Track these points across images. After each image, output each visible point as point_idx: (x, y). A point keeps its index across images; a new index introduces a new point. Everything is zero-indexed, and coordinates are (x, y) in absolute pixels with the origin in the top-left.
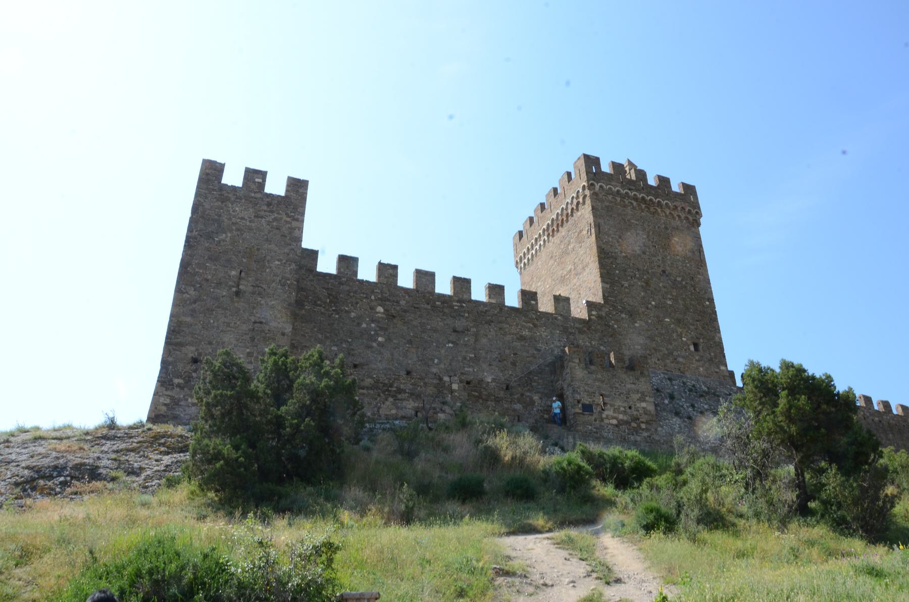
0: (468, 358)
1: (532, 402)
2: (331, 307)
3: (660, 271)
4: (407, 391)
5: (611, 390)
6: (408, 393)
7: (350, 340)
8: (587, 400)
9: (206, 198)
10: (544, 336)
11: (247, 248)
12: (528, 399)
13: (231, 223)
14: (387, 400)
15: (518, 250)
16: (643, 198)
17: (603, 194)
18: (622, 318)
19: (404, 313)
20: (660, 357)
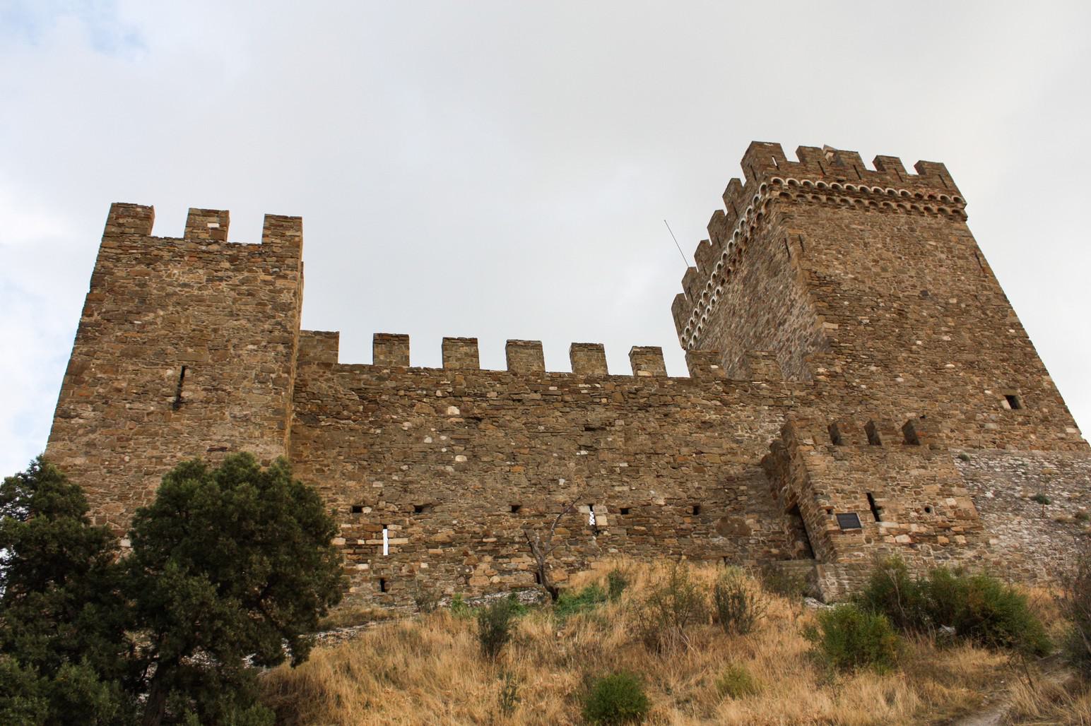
0: (618, 470)
1: (745, 531)
2: (367, 417)
3: (917, 292)
4: (517, 539)
5: (884, 483)
6: (518, 543)
7: (405, 467)
8: (843, 507)
9: (118, 260)
10: (742, 417)
11: (194, 330)
12: (736, 526)
13: (164, 294)
14: (480, 560)
17: (797, 193)
18: (872, 373)
19: (495, 412)
20: (953, 427)
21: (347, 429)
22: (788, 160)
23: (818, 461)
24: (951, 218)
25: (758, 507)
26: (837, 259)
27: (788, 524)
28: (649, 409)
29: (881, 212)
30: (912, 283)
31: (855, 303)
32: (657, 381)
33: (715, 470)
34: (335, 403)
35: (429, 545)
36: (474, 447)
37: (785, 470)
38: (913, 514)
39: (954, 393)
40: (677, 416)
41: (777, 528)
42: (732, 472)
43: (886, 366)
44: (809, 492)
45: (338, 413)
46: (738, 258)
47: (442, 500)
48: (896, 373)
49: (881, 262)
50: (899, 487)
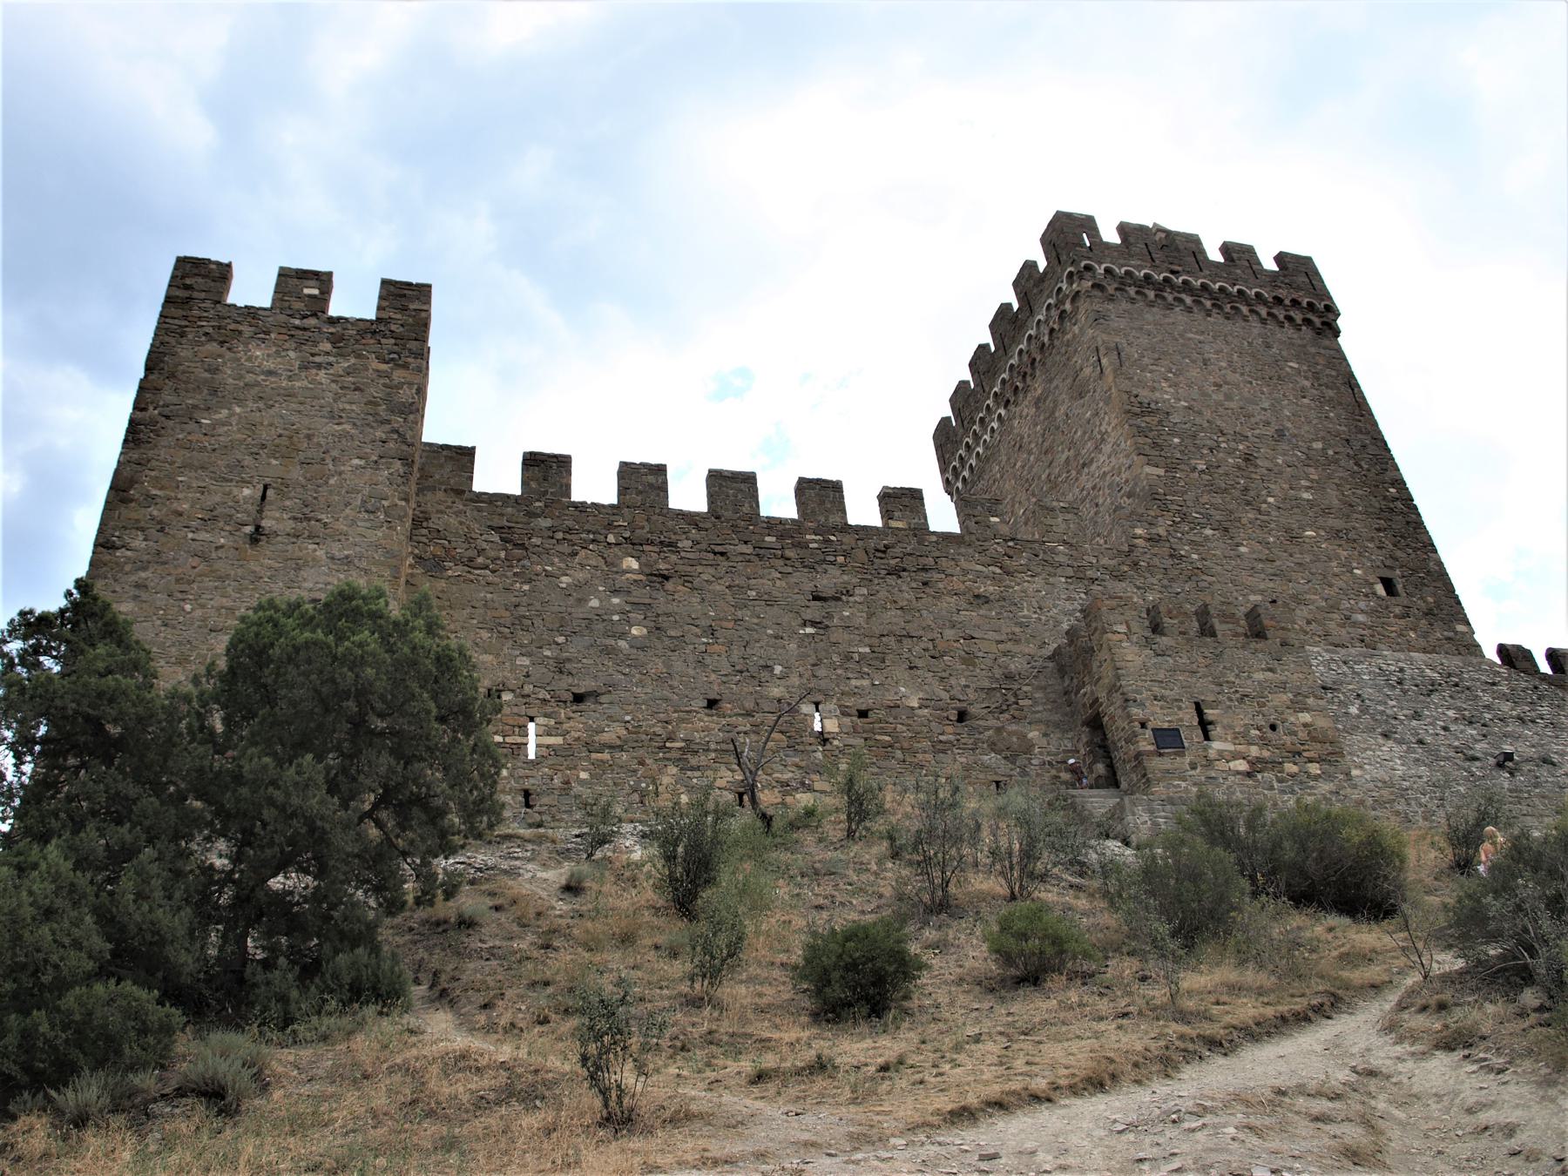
0: (856, 657)
1: (1028, 748)
3: (1270, 431)
4: (713, 746)
5: (1218, 689)
6: (716, 750)
7: (561, 639)
8: (1161, 718)
12: (1015, 739)
16: (1204, 287)
18: (1207, 538)
19: (689, 569)
20: (1310, 617)
21: (483, 582)
22: (1105, 239)
23: (1132, 655)
24: (1319, 332)
25: (1045, 715)
26: (1166, 380)
27: (1085, 740)
28: (902, 574)
29: (1228, 318)
34: (466, 546)
35: (589, 747)
36: (658, 615)
37: (1085, 666)
38: (1254, 732)
39: (1314, 570)
40: (941, 585)
41: (1069, 745)
42: (1012, 666)
44: (1117, 697)
45: (471, 560)
46: (1029, 371)
47: (611, 687)
49: (1225, 388)
50: (1238, 695)
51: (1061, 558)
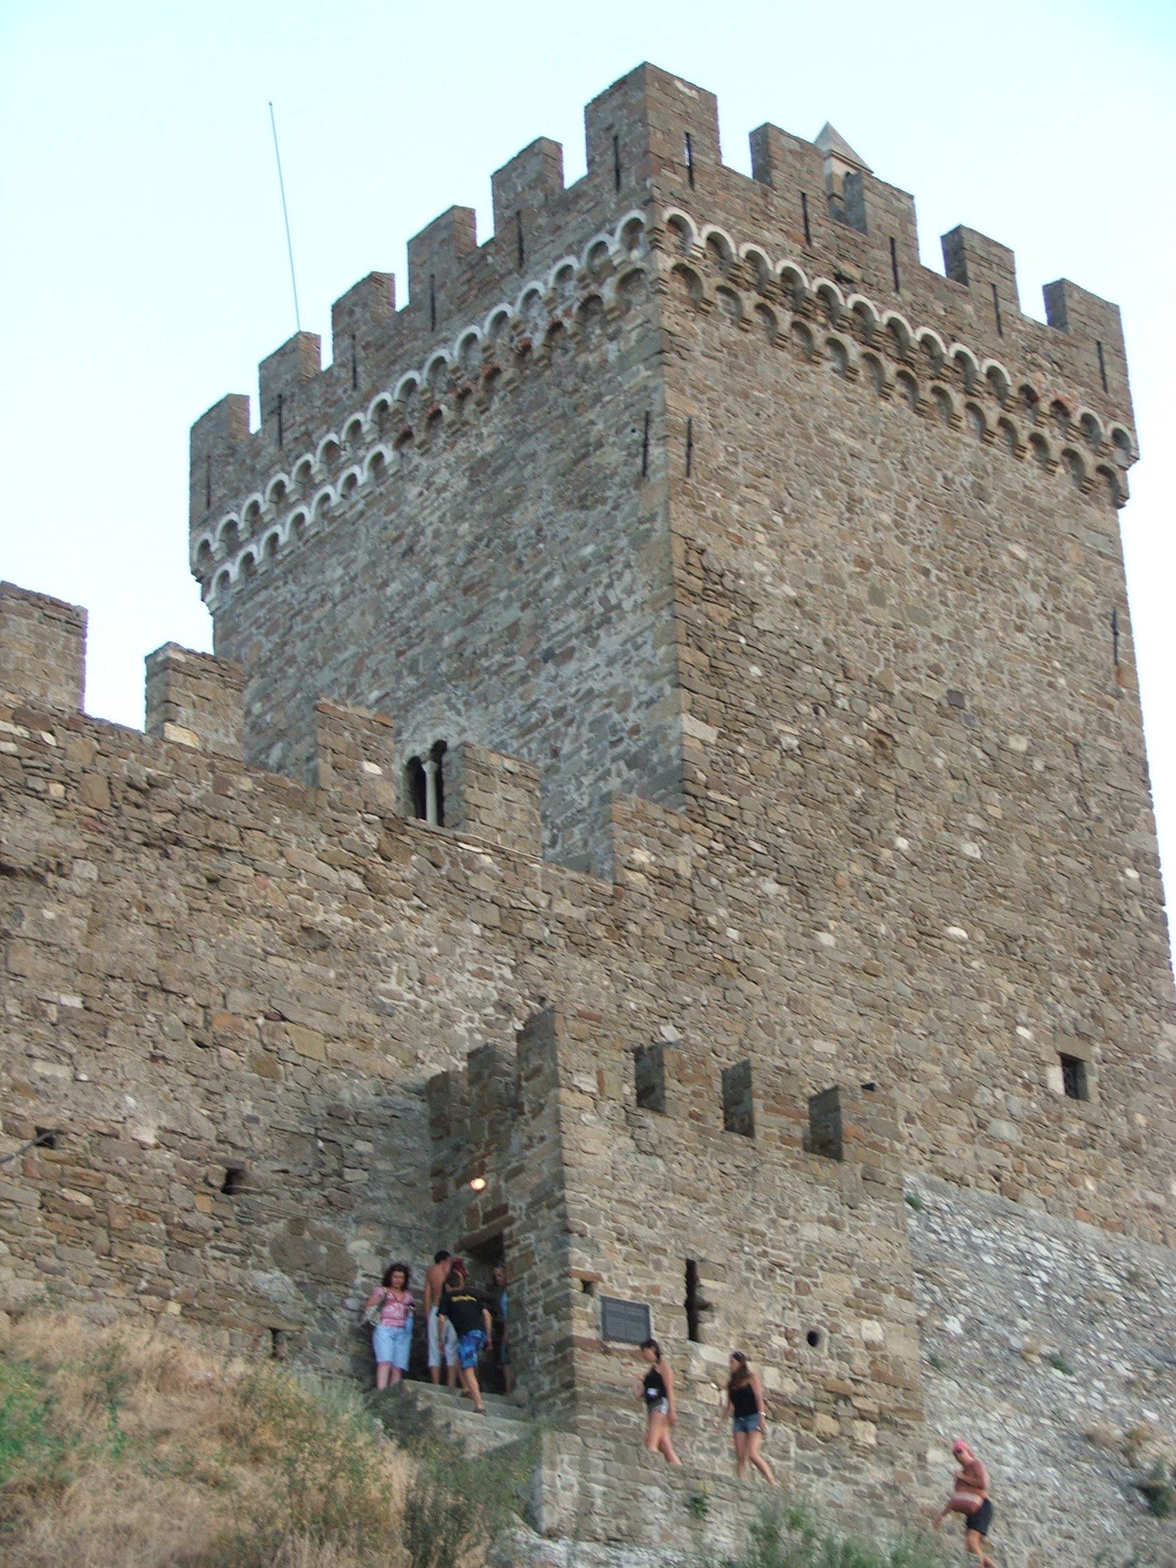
3: (937, 692)
5: (733, 1243)
12: (323, 1250)
15: (219, 492)
18: (764, 900)
22: (725, 162)
24: (1084, 484)
29: (919, 412)
30: (932, 660)
31: (777, 679)
32: (212, 767)
33: (304, 1076)
37: (493, 1132)
38: (779, 1342)
39: (945, 1013)
40: (242, 891)
42: (346, 1095)
43: (803, 891)
46: (478, 393)
48: (821, 916)
49: (877, 571)
50: (765, 1262)
51: (481, 883)
